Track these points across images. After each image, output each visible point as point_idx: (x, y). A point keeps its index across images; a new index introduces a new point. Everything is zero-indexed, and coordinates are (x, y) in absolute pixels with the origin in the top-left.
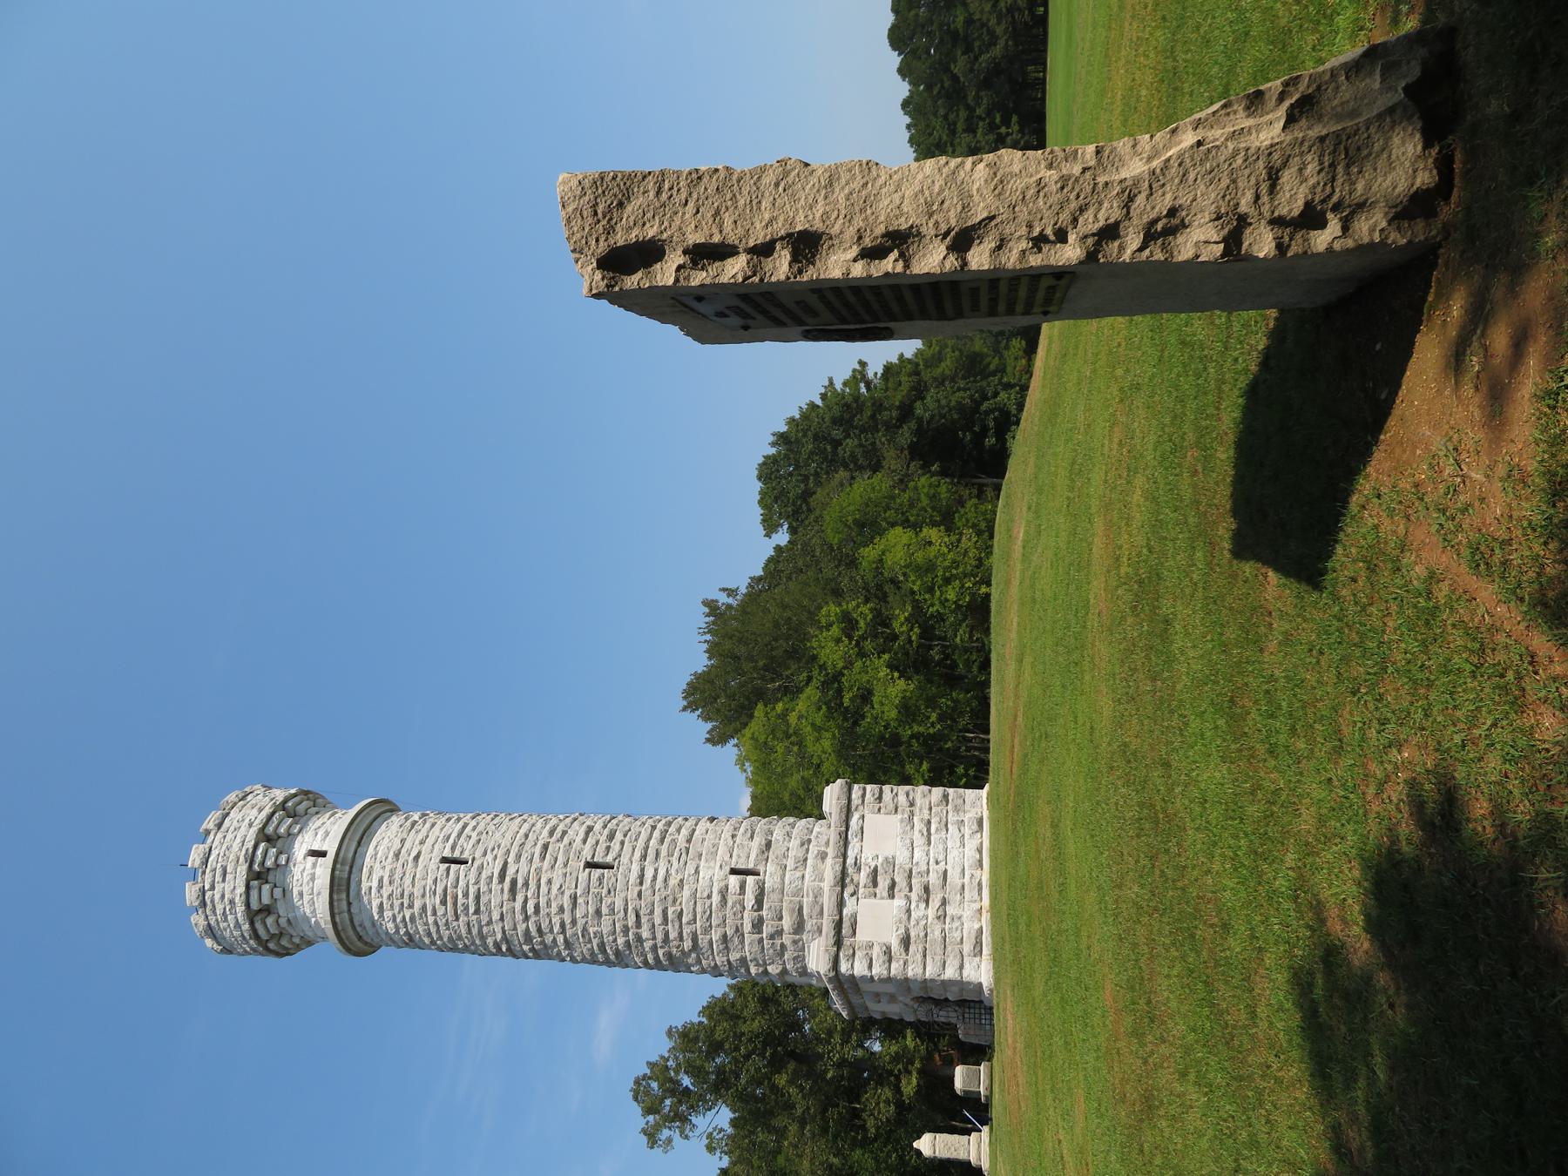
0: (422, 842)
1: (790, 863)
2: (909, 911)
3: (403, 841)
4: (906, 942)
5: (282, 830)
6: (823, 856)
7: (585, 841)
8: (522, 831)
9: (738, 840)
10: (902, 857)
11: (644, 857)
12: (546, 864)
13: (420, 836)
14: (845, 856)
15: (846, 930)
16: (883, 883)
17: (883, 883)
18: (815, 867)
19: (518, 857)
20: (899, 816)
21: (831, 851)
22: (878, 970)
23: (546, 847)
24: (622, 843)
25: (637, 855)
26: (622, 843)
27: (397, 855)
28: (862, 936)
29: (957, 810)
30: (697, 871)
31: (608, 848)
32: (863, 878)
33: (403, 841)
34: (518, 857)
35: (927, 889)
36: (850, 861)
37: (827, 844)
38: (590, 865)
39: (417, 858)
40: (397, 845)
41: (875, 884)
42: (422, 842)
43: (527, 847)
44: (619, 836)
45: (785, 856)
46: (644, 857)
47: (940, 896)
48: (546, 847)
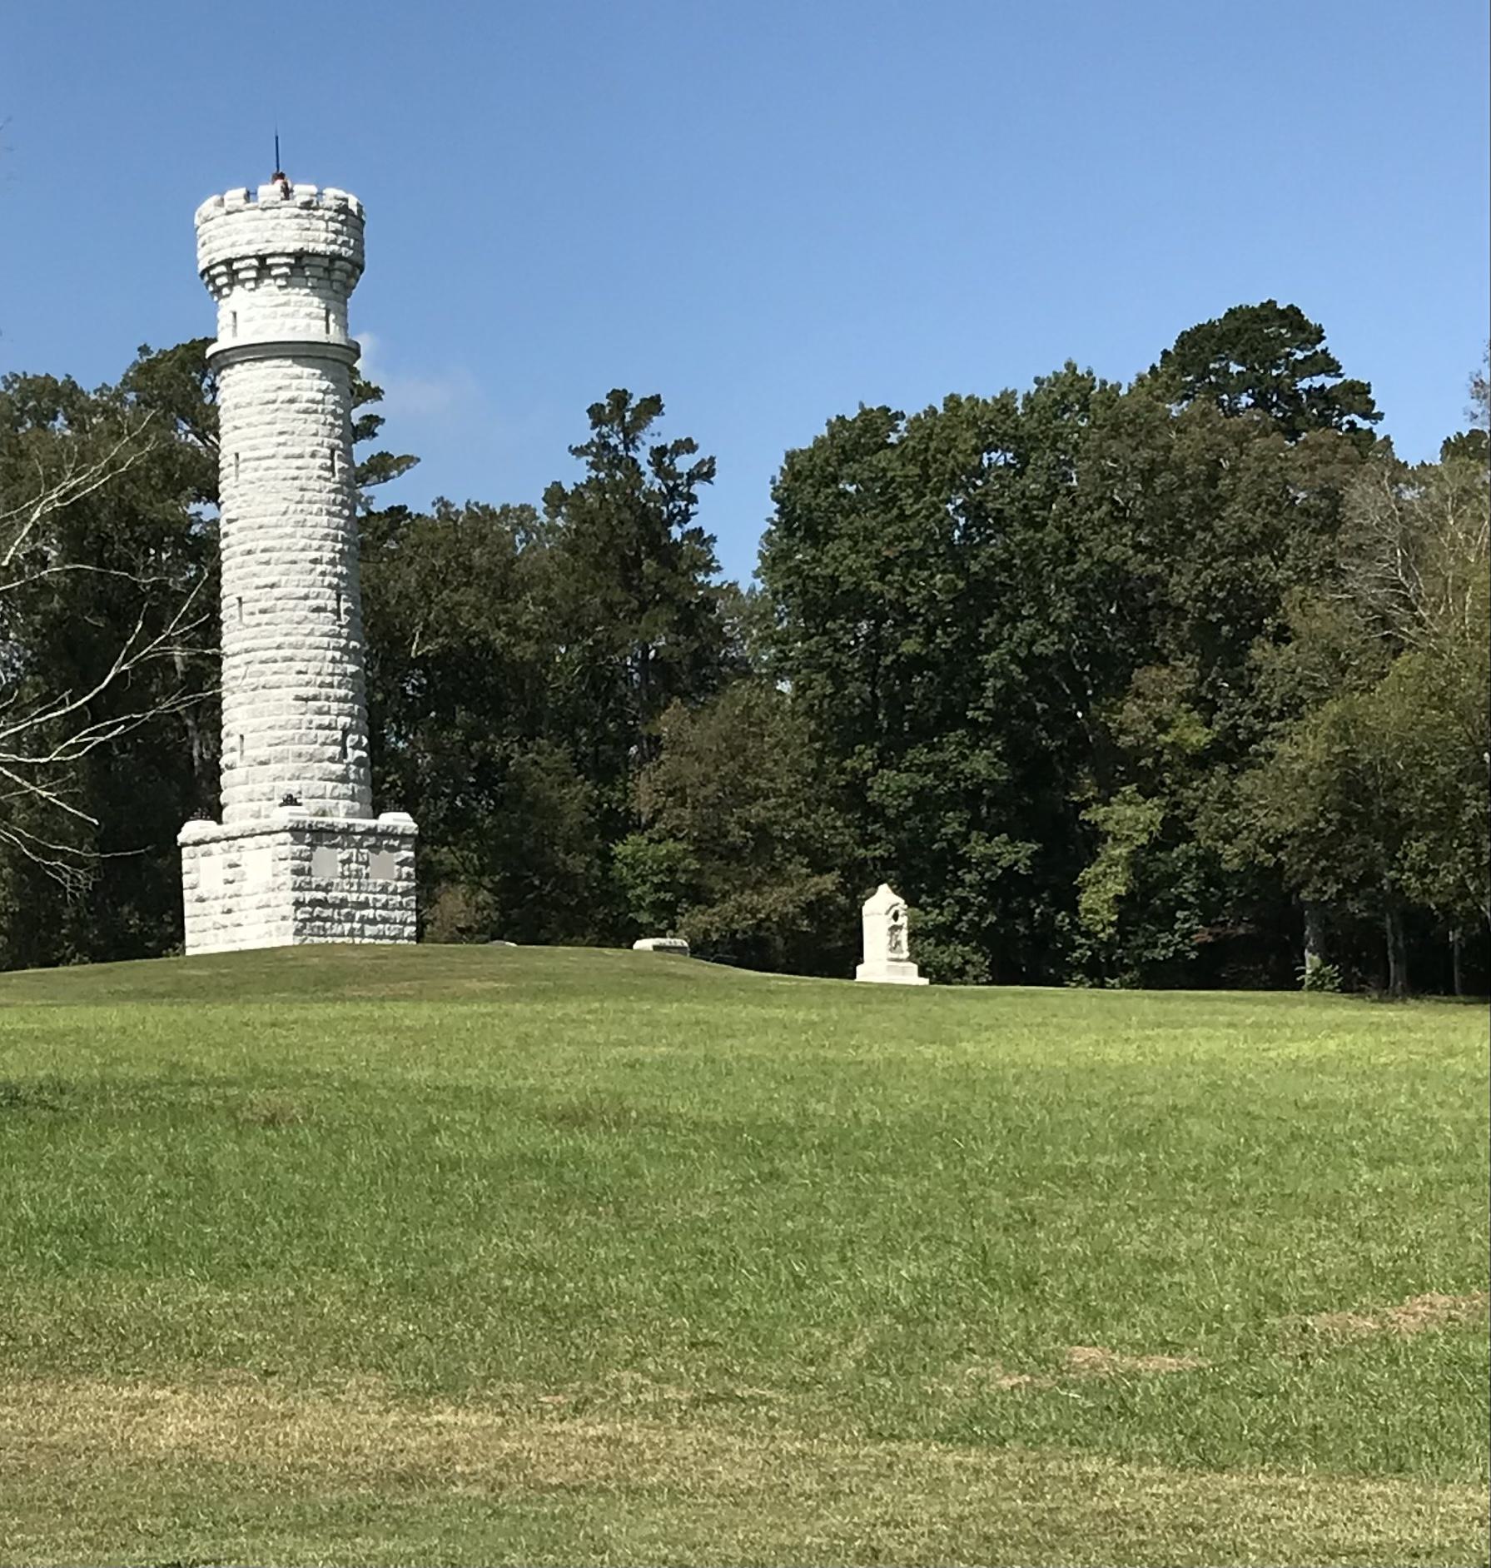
0: (249, 425)
1: (247, 788)
2: (217, 898)
3: (250, 404)
4: (201, 900)
5: (242, 275)
6: (257, 815)
7: (257, 588)
8: (265, 521)
9: (270, 732)
10: (247, 887)
11: (247, 651)
12: (240, 559)
13: (253, 420)
14: (242, 836)
15: (203, 847)
16: (230, 874)
17: (230, 874)
18: (246, 811)
19: (241, 530)
20: (271, 879)
21: (263, 821)
22: (187, 880)
23: (249, 552)
24: (259, 625)
25: (247, 644)
26: (259, 625)
27: (236, 407)
28: (203, 862)
29: (278, 928)
30: (240, 704)
31: (252, 614)
32: (233, 857)
33: (250, 404)
34: (241, 530)
35: (229, 911)
36: (241, 841)
37: (267, 816)
38: (240, 599)
39: (236, 428)
40: (243, 400)
41: (231, 866)
42: (249, 425)
43: (250, 534)
44: (266, 618)
45: (254, 781)
46: (247, 651)
47: (227, 923)
48: (249, 552)
